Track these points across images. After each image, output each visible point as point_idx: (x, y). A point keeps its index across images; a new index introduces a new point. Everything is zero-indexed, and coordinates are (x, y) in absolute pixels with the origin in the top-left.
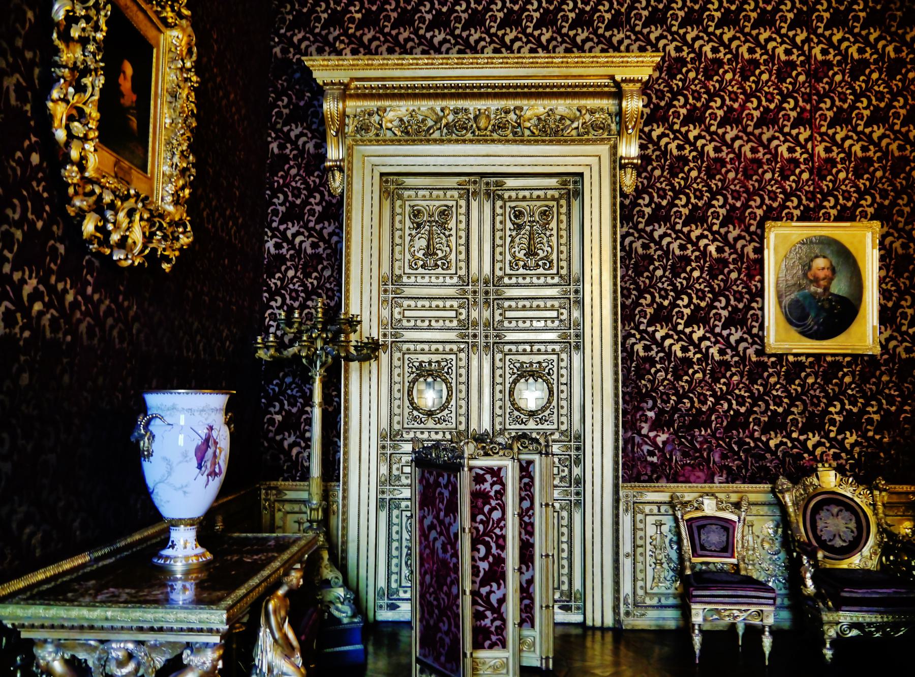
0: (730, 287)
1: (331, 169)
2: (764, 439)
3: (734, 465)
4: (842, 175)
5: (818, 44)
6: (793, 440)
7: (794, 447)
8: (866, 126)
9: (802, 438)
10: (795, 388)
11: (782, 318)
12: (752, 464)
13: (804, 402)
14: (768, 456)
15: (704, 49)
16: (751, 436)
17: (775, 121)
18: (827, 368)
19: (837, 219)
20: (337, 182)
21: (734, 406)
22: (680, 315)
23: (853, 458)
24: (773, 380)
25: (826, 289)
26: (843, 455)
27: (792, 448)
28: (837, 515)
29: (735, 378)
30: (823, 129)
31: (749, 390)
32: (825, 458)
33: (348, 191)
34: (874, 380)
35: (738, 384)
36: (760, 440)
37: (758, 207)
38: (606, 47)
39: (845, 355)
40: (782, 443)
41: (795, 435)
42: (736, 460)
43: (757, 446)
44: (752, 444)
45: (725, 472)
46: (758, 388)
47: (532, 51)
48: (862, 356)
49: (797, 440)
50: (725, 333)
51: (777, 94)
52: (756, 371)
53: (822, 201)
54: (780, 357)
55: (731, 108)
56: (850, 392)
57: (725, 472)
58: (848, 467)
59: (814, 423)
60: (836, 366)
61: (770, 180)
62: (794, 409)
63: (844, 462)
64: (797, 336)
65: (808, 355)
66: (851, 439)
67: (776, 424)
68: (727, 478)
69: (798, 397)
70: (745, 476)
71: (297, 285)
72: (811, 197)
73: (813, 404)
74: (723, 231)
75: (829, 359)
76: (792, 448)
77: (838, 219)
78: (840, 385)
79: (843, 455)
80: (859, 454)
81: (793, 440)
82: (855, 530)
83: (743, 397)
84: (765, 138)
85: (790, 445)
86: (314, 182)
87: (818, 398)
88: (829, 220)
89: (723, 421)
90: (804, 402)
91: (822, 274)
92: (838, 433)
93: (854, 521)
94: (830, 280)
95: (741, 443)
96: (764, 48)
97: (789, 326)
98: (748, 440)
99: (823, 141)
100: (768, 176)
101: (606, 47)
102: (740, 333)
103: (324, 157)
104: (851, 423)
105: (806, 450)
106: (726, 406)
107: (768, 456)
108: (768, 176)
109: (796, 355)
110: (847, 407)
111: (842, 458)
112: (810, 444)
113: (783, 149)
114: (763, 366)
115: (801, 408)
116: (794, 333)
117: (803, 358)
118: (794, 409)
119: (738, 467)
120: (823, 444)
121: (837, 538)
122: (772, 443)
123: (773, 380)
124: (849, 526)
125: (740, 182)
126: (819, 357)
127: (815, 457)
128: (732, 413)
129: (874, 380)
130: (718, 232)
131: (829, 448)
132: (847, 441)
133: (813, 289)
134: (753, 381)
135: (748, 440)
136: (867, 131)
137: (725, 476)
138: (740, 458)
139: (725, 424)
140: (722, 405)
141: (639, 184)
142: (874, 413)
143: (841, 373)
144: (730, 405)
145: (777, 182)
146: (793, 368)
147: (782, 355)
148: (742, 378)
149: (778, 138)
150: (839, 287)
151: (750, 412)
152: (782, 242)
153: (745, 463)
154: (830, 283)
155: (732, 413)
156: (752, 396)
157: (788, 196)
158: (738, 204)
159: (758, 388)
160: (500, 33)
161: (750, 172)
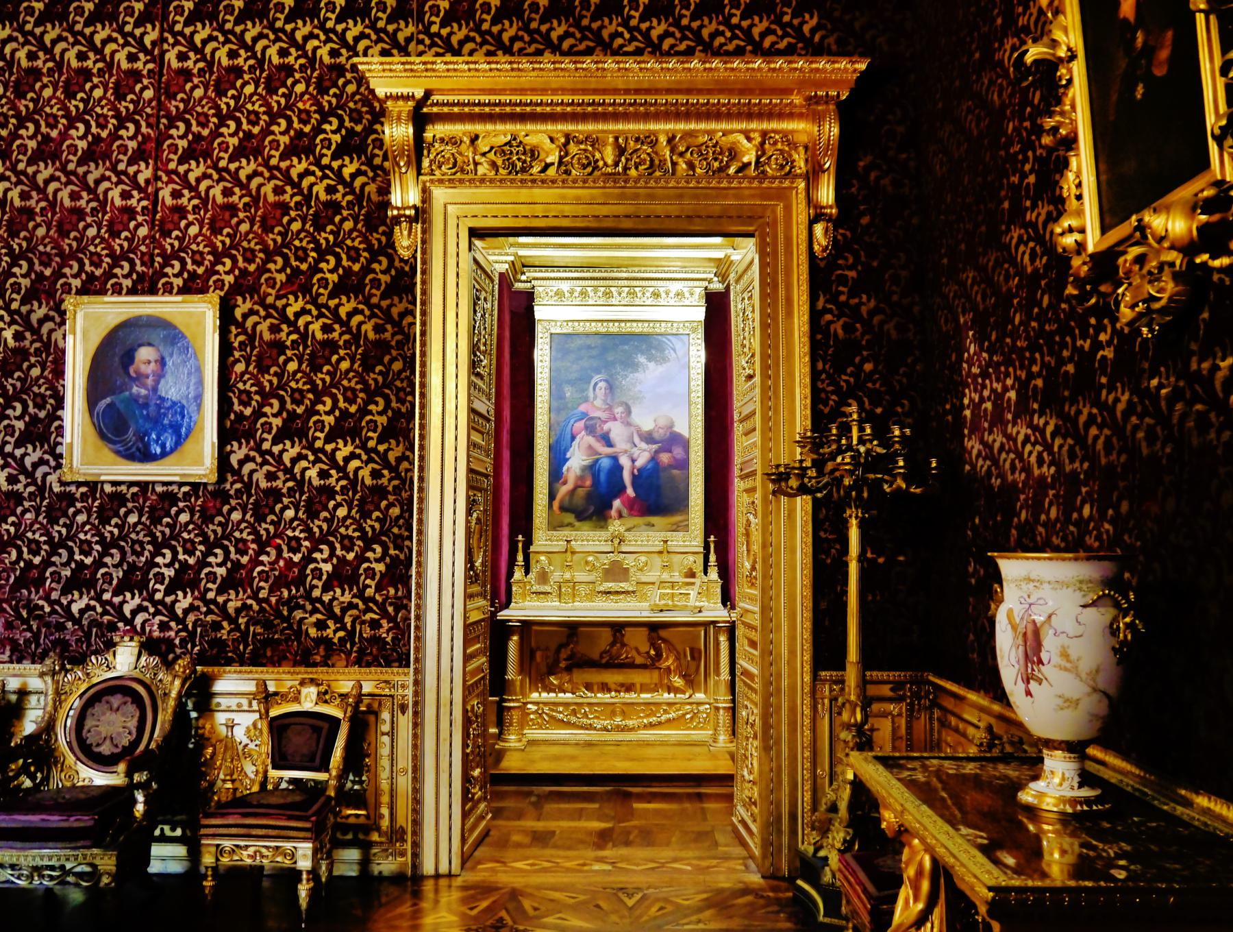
0: (30, 388)
1: (396, 220)
2: (65, 602)
3: (22, 637)
4: (193, 230)
5: (173, 46)
6: (103, 604)
7: (105, 613)
8: (282, 158)
9: (117, 600)
10: (111, 530)
11: (91, 431)
12: (46, 637)
13: (122, 550)
14: (69, 625)
15: (18, 54)
16: (47, 598)
17: (106, 155)
18: (160, 502)
19: (132, 291)
20: (404, 241)
21: (26, 556)
22: (267, 427)
23: (185, 629)
24: (81, 518)
25: (155, 389)
26: (173, 624)
27: (102, 615)
28: (118, 709)
29: (28, 516)
30: (172, 166)
31: (47, 533)
32: (148, 629)
33: (424, 252)
34: (169, 520)
35: (32, 525)
36: (58, 602)
37: (75, 276)
38: (493, 48)
39: (181, 484)
40: (88, 608)
41: (107, 596)
42: (24, 630)
43: (53, 611)
44: (47, 609)
45: (8, 648)
46: (59, 530)
47: (384, 53)
48: (205, 484)
49: (109, 603)
50: (18, 452)
51: (113, 117)
52: (60, 504)
53: (163, 266)
54: (93, 486)
55: (47, 138)
56: (185, 535)
57: (8, 648)
58: (177, 641)
59: (134, 581)
60: (169, 498)
61: (94, 238)
62: (107, 560)
63: (172, 634)
64: (112, 456)
65: (131, 484)
66: (184, 602)
67: (81, 581)
68: (10, 657)
69: (114, 543)
70: (34, 655)
71: (301, 383)
72: (148, 260)
73: (134, 552)
74: (24, 309)
75: (159, 489)
76: (102, 615)
77: (183, 291)
78: (172, 526)
79: (173, 624)
80: (195, 624)
81: (103, 604)
82: (134, 731)
83: (38, 542)
84: (91, 179)
85: (99, 610)
86: (223, 242)
87: (141, 543)
88: (171, 293)
89: (9, 577)
90: (122, 550)
91: (145, 369)
92: (167, 593)
93: (136, 719)
94: (160, 376)
95: (33, 608)
96: (301, 47)
97: (100, 443)
98: (41, 602)
99: (171, 181)
100: (92, 232)
101: (493, 48)
102: (39, 453)
103: (387, 204)
104: (184, 580)
105: (122, 617)
106: (14, 554)
107: (69, 625)
108: (92, 232)
109: (114, 484)
110: (181, 557)
111: (171, 629)
112: (127, 610)
113: (115, 194)
114: (69, 499)
115: (117, 558)
116: (107, 453)
117: (123, 488)
118: (107, 560)
119: (27, 641)
120: (146, 609)
121: (108, 742)
122: (75, 608)
123: (81, 518)
124: (129, 725)
125: (53, 240)
126: (144, 486)
127: (134, 627)
128: (22, 564)
129: (221, 519)
130: (18, 312)
131: (154, 615)
132: (177, 605)
133: (135, 389)
134: (53, 521)
135: (41, 602)
136: (284, 165)
137: (8, 653)
138: (30, 629)
139: (12, 580)
140: (9, 554)
141: (839, 237)
142: (166, 566)
143: (175, 509)
144: (20, 553)
145: (103, 240)
146: (111, 502)
147: (147, 483)
148: (37, 517)
149: (109, 179)
150: (172, 390)
151: (47, 563)
152: (86, 325)
153: (36, 636)
154: (157, 382)
155: (22, 564)
156: (50, 541)
157: (116, 260)
158: (48, 272)
159: (59, 530)
160: (138, 32)
161: (67, 227)
